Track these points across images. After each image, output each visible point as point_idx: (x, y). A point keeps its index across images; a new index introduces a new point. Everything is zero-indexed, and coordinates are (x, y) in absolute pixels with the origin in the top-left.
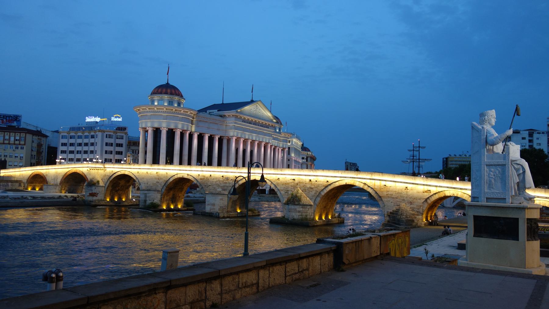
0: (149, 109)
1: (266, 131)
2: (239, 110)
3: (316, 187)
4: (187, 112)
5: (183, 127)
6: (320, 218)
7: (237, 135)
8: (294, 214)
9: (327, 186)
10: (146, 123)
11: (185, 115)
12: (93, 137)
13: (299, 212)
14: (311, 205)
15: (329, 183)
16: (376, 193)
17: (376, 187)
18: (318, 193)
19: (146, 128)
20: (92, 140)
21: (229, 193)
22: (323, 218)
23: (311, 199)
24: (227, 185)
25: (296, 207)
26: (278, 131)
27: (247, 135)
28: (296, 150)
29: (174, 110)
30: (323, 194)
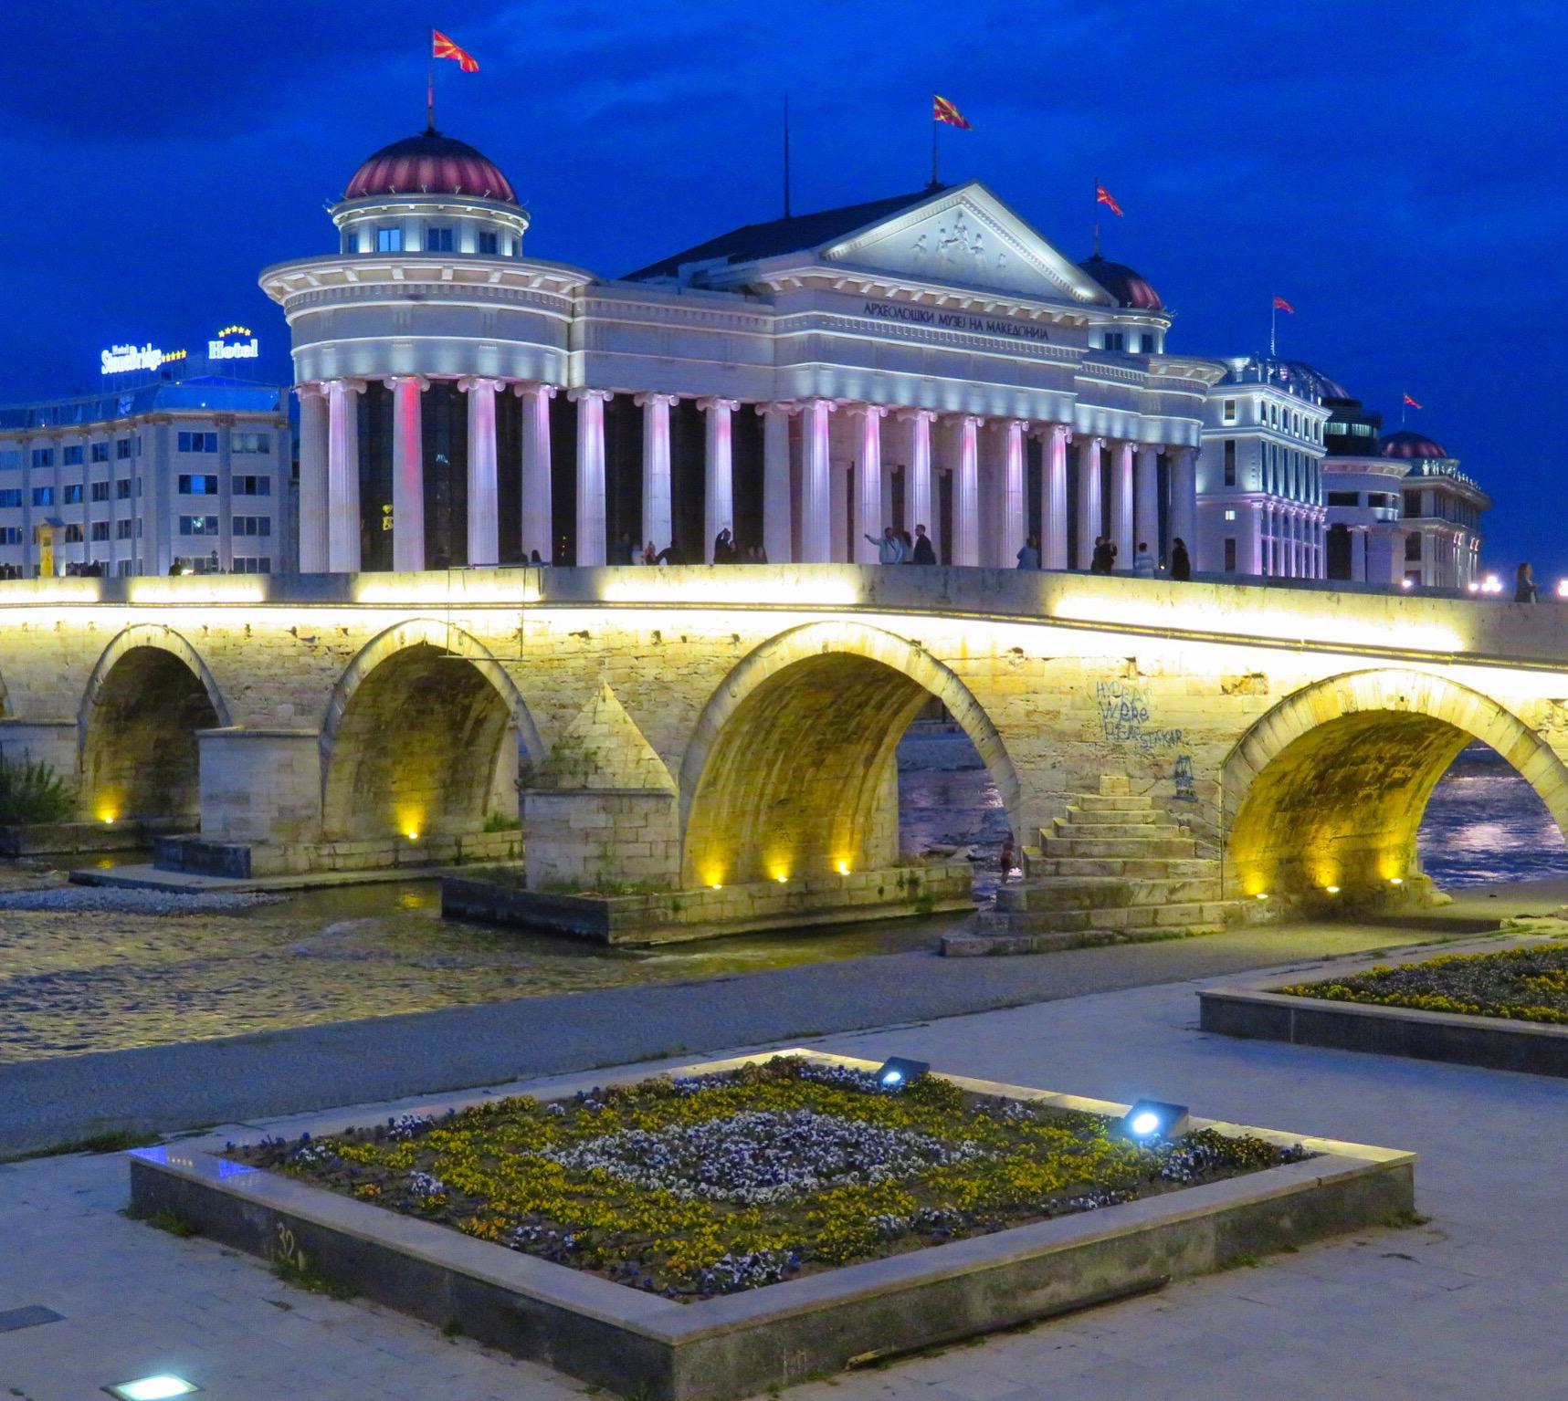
0: (324, 280)
1: (1027, 353)
2: (839, 249)
3: (685, 679)
4: (527, 281)
5: (507, 366)
6: (748, 873)
7: (840, 392)
8: (552, 850)
9: (734, 673)
10: (316, 354)
11: (516, 298)
12: (125, 450)
13: (586, 836)
14: (660, 795)
15: (742, 650)
16: (974, 704)
17: (972, 665)
18: (694, 715)
19: (317, 387)
20: (122, 470)
21: (325, 729)
22: (779, 872)
23: (664, 755)
24: (314, 677)
25: (567, 807)
26: (1134, 348)
27: (904, 387)
28: (1276, 460)
29: (447, 275)
30: (720, 718)
